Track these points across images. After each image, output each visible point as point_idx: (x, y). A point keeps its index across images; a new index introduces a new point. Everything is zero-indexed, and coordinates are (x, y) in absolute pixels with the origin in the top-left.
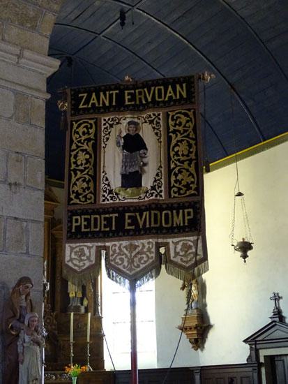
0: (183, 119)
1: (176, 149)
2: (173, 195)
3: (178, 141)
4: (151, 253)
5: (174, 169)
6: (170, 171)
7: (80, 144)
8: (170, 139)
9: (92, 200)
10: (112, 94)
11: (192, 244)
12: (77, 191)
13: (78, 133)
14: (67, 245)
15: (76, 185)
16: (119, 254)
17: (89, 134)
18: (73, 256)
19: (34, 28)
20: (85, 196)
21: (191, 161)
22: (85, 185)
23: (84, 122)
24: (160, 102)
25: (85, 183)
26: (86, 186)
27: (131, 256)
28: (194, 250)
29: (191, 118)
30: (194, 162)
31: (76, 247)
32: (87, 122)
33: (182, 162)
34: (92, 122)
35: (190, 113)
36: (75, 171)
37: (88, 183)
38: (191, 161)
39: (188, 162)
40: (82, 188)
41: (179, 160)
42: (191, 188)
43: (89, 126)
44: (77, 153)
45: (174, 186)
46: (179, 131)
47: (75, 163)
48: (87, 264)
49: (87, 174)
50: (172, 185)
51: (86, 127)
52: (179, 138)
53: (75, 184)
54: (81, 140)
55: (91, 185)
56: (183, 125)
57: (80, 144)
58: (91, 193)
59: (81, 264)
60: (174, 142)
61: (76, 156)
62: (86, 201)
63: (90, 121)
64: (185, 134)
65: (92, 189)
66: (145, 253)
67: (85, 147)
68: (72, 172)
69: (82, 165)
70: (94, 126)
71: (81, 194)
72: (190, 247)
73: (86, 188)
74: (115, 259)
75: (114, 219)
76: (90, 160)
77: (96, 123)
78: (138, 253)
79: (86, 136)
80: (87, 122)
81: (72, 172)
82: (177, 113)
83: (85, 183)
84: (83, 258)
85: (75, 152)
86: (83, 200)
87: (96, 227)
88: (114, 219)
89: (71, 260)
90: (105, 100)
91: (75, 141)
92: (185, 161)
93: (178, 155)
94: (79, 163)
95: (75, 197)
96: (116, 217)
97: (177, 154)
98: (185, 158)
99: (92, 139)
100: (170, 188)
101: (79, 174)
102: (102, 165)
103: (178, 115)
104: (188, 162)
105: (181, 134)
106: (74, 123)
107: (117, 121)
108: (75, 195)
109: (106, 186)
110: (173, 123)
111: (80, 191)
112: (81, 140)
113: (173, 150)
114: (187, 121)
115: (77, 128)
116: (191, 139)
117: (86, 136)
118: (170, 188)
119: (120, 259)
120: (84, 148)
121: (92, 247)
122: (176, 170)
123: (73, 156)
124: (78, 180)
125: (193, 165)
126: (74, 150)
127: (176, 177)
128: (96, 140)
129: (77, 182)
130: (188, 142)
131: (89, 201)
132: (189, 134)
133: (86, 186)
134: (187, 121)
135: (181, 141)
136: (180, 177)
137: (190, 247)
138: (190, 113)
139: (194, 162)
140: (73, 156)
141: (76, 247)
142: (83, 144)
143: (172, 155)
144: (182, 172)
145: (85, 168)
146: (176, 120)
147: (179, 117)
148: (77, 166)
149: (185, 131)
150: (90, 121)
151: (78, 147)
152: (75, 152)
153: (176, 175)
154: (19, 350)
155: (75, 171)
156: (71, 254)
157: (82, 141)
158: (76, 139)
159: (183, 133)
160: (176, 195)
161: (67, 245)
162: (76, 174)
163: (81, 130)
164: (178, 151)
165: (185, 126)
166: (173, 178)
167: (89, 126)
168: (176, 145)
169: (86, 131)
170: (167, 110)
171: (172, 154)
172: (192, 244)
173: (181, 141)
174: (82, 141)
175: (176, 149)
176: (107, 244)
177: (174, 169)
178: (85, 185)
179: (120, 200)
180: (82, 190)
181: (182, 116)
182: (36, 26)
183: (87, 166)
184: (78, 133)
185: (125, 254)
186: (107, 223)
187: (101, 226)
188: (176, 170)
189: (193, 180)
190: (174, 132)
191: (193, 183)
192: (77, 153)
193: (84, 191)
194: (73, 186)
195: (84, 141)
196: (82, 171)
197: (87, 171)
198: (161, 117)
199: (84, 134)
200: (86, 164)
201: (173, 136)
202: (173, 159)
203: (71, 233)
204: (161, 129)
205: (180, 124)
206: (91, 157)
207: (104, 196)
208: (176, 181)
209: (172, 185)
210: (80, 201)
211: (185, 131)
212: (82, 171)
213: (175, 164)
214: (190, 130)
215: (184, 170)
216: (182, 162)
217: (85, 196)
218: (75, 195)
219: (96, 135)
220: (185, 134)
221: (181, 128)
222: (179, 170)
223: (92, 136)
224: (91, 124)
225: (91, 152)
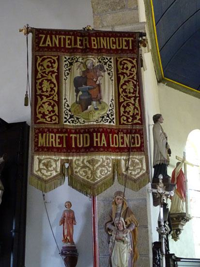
0: (130, 65)
1: (124, 87)
2: (122, 121)
3: (125, 82)
4: (109, 167)
5: (122, 102)
6: (120, 104)
7: (44, 75)
8: (119, 80)
9: (57, 121)
10: (61, 38)
11: (138, 161)
12: (44, 112)
13: (42, 65)
14: (36, 157)
15: (43, 107)
16: (83, 167)
17: (53, 68)
18: (41, 166)
19: (123, 8)
20: (51, 117)
21: (135, 97)
22: (50, 108)
23: (48, 58)
24: (119, 50)
25: (50, 106)
26: (52, 109)
27: (93, 169)
28: (140, 166)
29: (135, 65)
30: (138, 98)
31: (44, 159)
32: (51, 58)
33: (130, 98)
34: (55, 58)
35: (134, 61)
36: (41, 96)
37: (53, 107)
38: (135, 97)
39: (133, 98)
40: (48, 110)
41: (126, 96)
42: (136, 118)
43: (52, 61)
44: (42, 81)
45: (123, 115)
46: (127, 74)
47: (41, 89)
48: (54, 174)
49: (52, 99)
50: (121, 115)
51: (50, 61)
52: (126, 79)
53: (42, 106)
54: (45, 72)
55: (56, 108)
56: (129, 70)
57: (44, 75)
58: (55, 115)
59: (49, 173)
60: (122, 82)
61: (41, 84)
62: (51, 121)
63: (53, 58)
64: (131, 77)
65: (56, 112)
66: (104, 166)
67: (49, 77)
68: (38, 97)
69: (47, 91)
70: (56, 61)
71: (47, 115)
72: (137, 164)
73: (51, 111)
74: (79, 172)
75: (64, 139)
76: (55, 88)
77: (58, 59)
78: (100, 166)
79: (51, 69)
80: (51, 58)
81: (38, 97)
82: (124, 60)
83: (50, 106)
84: (50, 169)
85: (40, 80)
86: (49, 120)
87: (116, 145)
88: (64, 139)
89: (40, 170)
90: (55, 39)
91: (40, 72)
92: (132, 97)
93: (126, 92)
94: (44, 89)
95: (42, 117)
96: (66, 136)
97: (124, 91)
98: (131, 95)
99: (56, 72)
100: (120, 117)
101: (45, 99)
102: (64, 94)
103: (125, 61)
104: (133, 98)
105: (128, 76)
106: (38, 57)
107: (76, 60)
108: (41, 115)
109: (68, 111)
110: (121, 67)
111: (47, 113)
112: (45, 72)
113: (122, 87)
114: (132, 67)
115: (42, 61)
116: (135, 80)
117: (51, 69)
118: (120, 117)
119: (84, 171)
120: (49, 78)
121: (58, 160)
122: (125, 103)
123: (38, 84)
124: (44, 103)
125: (137, 101)
126: (39, 79)
127: (125, 109)
128: (58, 73)
129: (43, 105)
130: (133, 83)
131: (53, 122)
132: (133, 77)
133: (52, 109)
134: (132, 67)
135: (128, 81)
136: (128, 109)
137: (137, 164)
138: (134, 61)
139: (138, 98)
140: (38, 84)
141: (44, 159)
142: (47, 75)
143: (121, 92)
144: (130, 105)
145: (51, 95)
146: (124, 65)
147: (125, 63)
148: (43, 92)
149: (131, 74)
150: (53, 58)
151: (43, 76)
152: (40, 80)
153: (125, 107)
154: (167, 223)
155: (41, 96)
156: (39, 165)
157: (47, 73)
158: (41, 70)
159: (129, 76)
160: (125, 122)
161: (36, 157)
162: (42, 99)
163: (45, 63)
164: (126, 89)
165: (130, 71)
166: (122, 109)
167: (52, 61)
168: (124, 84)
169: (50, 65)
170: (118, 56)
171: (121, 90)
172: (138, 161)
173: (128, 81)
174: (47, 73)
175: (124, 87)
176: (70, 158)
177: (122, 102)
178: (50, 108)
179: (80, 123)
180: (48, 112)
181: (128, 62)
182: (124, 6)
183: (52, 93)
184: (42, 65)
185: (88, 167)
186: (60, 141)
187: (83, 144)
188: (125, 103)
189: (137, 112)
190: (123, 74)
191: (137, 114)
192: (42, 81)
193: (50, 113)
194: (39, 108)
195: (49, 72)
196: (47, 97)
197: (52, 97)
198: (112, 60)
199: (48, 66)
200: (51, 91)
201: (122, 77)
202: (122, 95)
203: (38, 147)
204: (112, 70)
205: (127, 68)
206: (55, 86)
207: (65, 118)
208: (125, 112)
209: (121, 115)
210: (46, 120)
211: (131, 74)
212: (47, 97)
213: (124, 99)
214: (135, 73)
215: (130, 104)
216: (130, 98)
217: (51, 117)
218: (41, 115)
219: (58, 69)
220: (131, 77)
221: (128, 72)
222: (127, 104)
223: (55, 70)
224: (54, 60)
225: (55, 82)
